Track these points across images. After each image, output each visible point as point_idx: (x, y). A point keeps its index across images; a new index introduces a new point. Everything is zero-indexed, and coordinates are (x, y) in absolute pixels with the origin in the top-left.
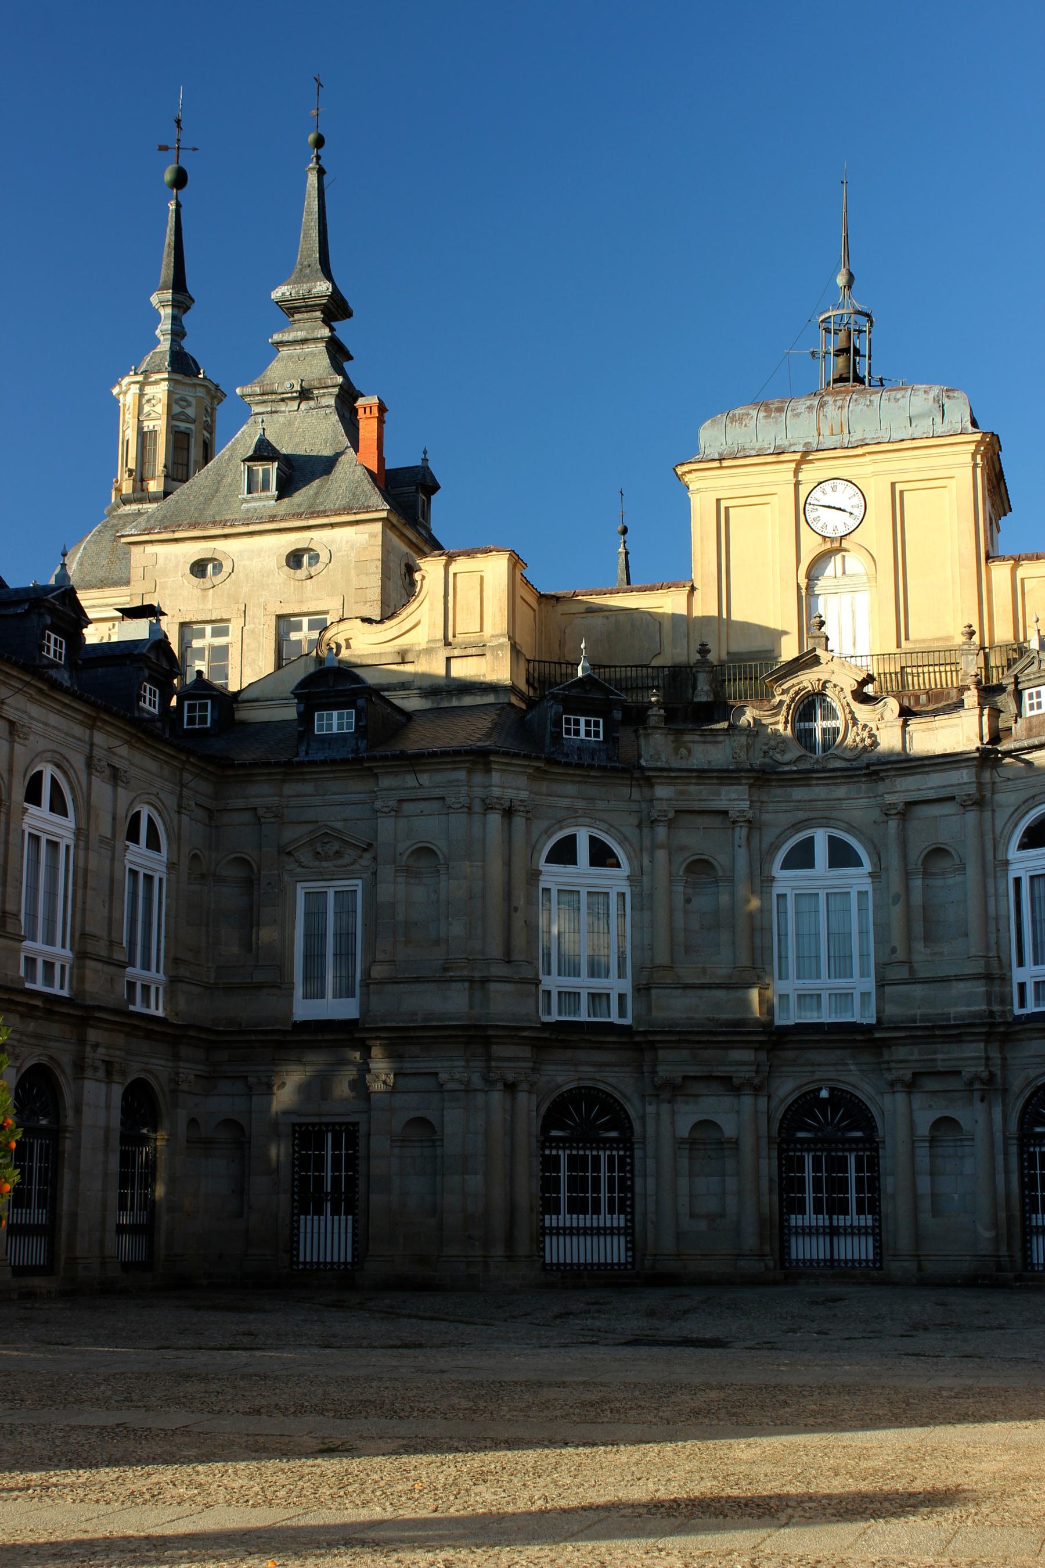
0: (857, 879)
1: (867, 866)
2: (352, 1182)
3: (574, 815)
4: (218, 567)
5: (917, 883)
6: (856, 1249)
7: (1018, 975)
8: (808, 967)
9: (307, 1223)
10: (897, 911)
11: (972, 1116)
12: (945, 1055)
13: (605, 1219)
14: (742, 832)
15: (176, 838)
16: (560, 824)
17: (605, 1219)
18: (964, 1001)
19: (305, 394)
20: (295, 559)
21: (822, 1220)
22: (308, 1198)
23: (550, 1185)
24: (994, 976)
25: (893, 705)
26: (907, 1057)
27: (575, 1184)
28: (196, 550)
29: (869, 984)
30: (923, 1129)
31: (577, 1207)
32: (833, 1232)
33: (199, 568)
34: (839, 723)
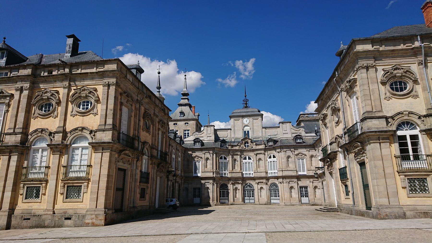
0: (251, 161)
1: (252, 160)
2: (200, 194)
3: (222, 154)
4: (177, 124)
5: (258, 162)
6: (253, 201)
7: (269, 172)
8: (246, 171)
9: (195, 199)
10: (256, 165)
11: (264, 186)
12: (261, 181)
13: (226, 198)
14: (239, 156)
15: (181, 156)
16: (221, 154)
17: (226, 198)
18: (263, 175)
19: (185, 105)
20: (186, 124)
21: (248, 198)
22: (195, 196)
23: (220, 194)
24: (267, 173)
25: (255, 144)
26: (257, 181)
27: (223, 194)
28: (174, 123)
29: (253, 172)
30: (259, 188)
31: (223, 197)
32: (250, 199)
33: (174, 124)
34: (249, 144)
